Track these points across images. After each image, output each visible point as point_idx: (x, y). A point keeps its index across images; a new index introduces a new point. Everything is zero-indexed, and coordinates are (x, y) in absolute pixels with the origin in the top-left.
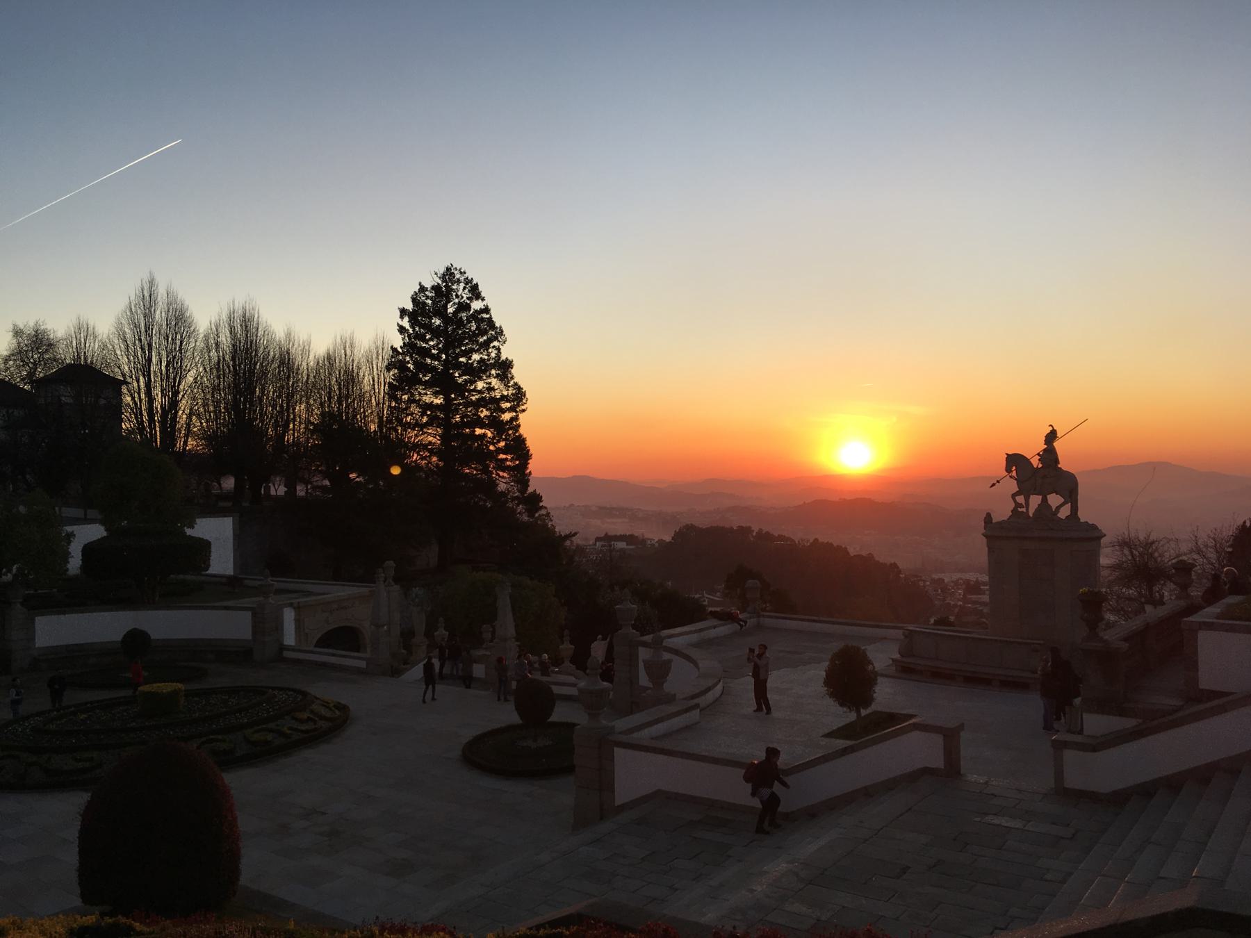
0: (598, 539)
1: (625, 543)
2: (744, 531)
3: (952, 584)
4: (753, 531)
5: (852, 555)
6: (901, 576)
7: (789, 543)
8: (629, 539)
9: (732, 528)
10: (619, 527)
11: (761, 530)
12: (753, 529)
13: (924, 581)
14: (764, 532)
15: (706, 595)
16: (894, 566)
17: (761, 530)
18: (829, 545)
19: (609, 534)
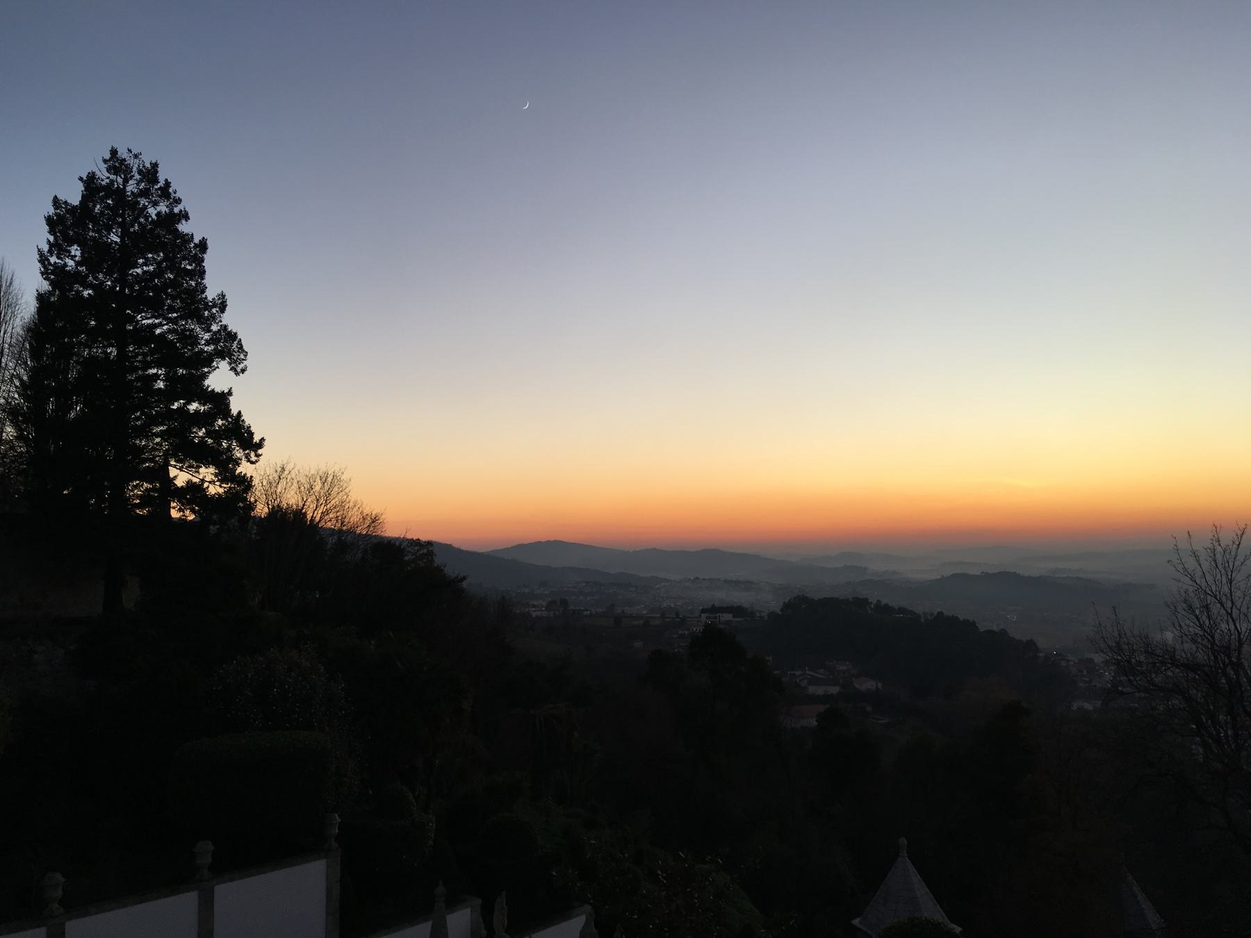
0: (703, 611)
1: (731, 615)
2: (862, 602)
3: (1102, 665)
4: (871, 603)
5: (981, 630)
6: (1041, 655)
7: (909, 616)
8: (737, 611)
9: (848, 600)
10: (722, 596)
11: (879, 601)
12: (870, 601)
13: (1068, 661)
14: (882, 604)
15: (807, 672)
16: (1031, 644)
17: (879, 601)
18: (953, 620)
19: (717, 604)
